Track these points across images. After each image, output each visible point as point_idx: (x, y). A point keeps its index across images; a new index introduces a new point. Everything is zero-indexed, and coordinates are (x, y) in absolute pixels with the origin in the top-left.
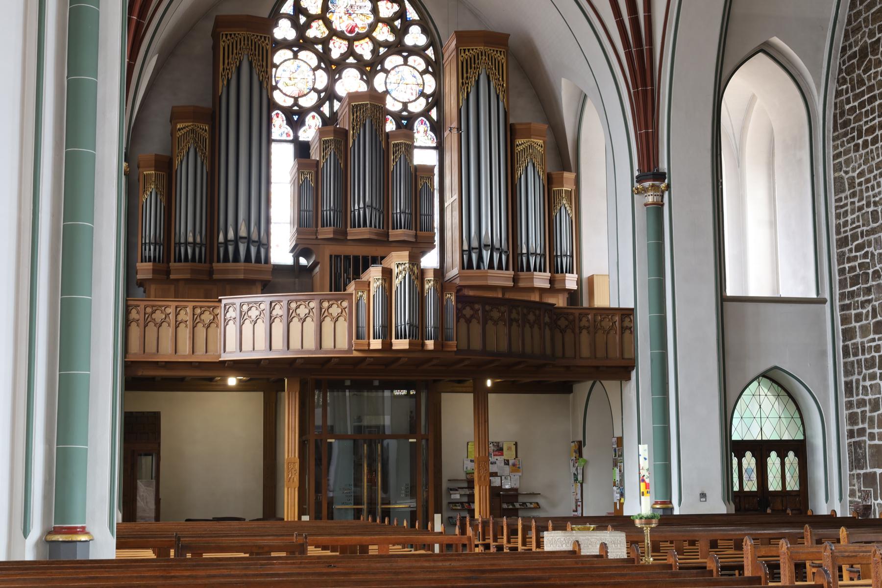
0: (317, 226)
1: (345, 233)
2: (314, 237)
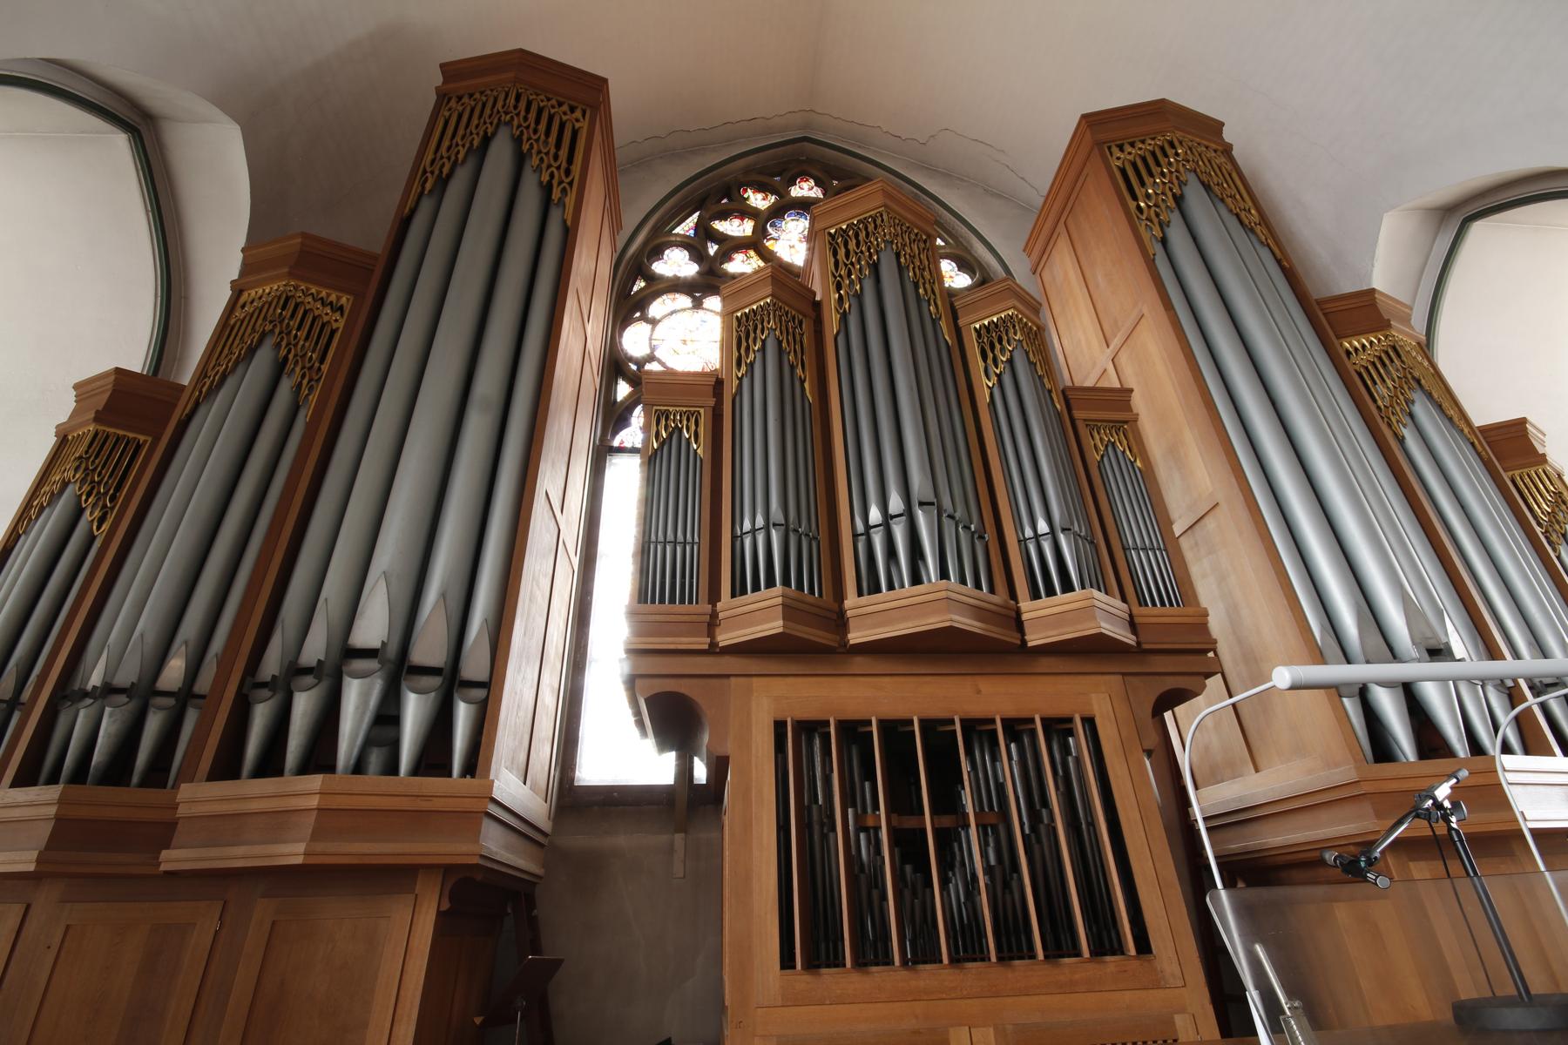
0: (714, 596)
1: (840, 622)
2: (702, 643)
